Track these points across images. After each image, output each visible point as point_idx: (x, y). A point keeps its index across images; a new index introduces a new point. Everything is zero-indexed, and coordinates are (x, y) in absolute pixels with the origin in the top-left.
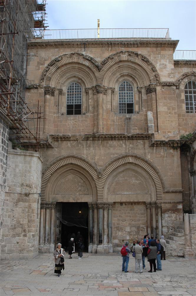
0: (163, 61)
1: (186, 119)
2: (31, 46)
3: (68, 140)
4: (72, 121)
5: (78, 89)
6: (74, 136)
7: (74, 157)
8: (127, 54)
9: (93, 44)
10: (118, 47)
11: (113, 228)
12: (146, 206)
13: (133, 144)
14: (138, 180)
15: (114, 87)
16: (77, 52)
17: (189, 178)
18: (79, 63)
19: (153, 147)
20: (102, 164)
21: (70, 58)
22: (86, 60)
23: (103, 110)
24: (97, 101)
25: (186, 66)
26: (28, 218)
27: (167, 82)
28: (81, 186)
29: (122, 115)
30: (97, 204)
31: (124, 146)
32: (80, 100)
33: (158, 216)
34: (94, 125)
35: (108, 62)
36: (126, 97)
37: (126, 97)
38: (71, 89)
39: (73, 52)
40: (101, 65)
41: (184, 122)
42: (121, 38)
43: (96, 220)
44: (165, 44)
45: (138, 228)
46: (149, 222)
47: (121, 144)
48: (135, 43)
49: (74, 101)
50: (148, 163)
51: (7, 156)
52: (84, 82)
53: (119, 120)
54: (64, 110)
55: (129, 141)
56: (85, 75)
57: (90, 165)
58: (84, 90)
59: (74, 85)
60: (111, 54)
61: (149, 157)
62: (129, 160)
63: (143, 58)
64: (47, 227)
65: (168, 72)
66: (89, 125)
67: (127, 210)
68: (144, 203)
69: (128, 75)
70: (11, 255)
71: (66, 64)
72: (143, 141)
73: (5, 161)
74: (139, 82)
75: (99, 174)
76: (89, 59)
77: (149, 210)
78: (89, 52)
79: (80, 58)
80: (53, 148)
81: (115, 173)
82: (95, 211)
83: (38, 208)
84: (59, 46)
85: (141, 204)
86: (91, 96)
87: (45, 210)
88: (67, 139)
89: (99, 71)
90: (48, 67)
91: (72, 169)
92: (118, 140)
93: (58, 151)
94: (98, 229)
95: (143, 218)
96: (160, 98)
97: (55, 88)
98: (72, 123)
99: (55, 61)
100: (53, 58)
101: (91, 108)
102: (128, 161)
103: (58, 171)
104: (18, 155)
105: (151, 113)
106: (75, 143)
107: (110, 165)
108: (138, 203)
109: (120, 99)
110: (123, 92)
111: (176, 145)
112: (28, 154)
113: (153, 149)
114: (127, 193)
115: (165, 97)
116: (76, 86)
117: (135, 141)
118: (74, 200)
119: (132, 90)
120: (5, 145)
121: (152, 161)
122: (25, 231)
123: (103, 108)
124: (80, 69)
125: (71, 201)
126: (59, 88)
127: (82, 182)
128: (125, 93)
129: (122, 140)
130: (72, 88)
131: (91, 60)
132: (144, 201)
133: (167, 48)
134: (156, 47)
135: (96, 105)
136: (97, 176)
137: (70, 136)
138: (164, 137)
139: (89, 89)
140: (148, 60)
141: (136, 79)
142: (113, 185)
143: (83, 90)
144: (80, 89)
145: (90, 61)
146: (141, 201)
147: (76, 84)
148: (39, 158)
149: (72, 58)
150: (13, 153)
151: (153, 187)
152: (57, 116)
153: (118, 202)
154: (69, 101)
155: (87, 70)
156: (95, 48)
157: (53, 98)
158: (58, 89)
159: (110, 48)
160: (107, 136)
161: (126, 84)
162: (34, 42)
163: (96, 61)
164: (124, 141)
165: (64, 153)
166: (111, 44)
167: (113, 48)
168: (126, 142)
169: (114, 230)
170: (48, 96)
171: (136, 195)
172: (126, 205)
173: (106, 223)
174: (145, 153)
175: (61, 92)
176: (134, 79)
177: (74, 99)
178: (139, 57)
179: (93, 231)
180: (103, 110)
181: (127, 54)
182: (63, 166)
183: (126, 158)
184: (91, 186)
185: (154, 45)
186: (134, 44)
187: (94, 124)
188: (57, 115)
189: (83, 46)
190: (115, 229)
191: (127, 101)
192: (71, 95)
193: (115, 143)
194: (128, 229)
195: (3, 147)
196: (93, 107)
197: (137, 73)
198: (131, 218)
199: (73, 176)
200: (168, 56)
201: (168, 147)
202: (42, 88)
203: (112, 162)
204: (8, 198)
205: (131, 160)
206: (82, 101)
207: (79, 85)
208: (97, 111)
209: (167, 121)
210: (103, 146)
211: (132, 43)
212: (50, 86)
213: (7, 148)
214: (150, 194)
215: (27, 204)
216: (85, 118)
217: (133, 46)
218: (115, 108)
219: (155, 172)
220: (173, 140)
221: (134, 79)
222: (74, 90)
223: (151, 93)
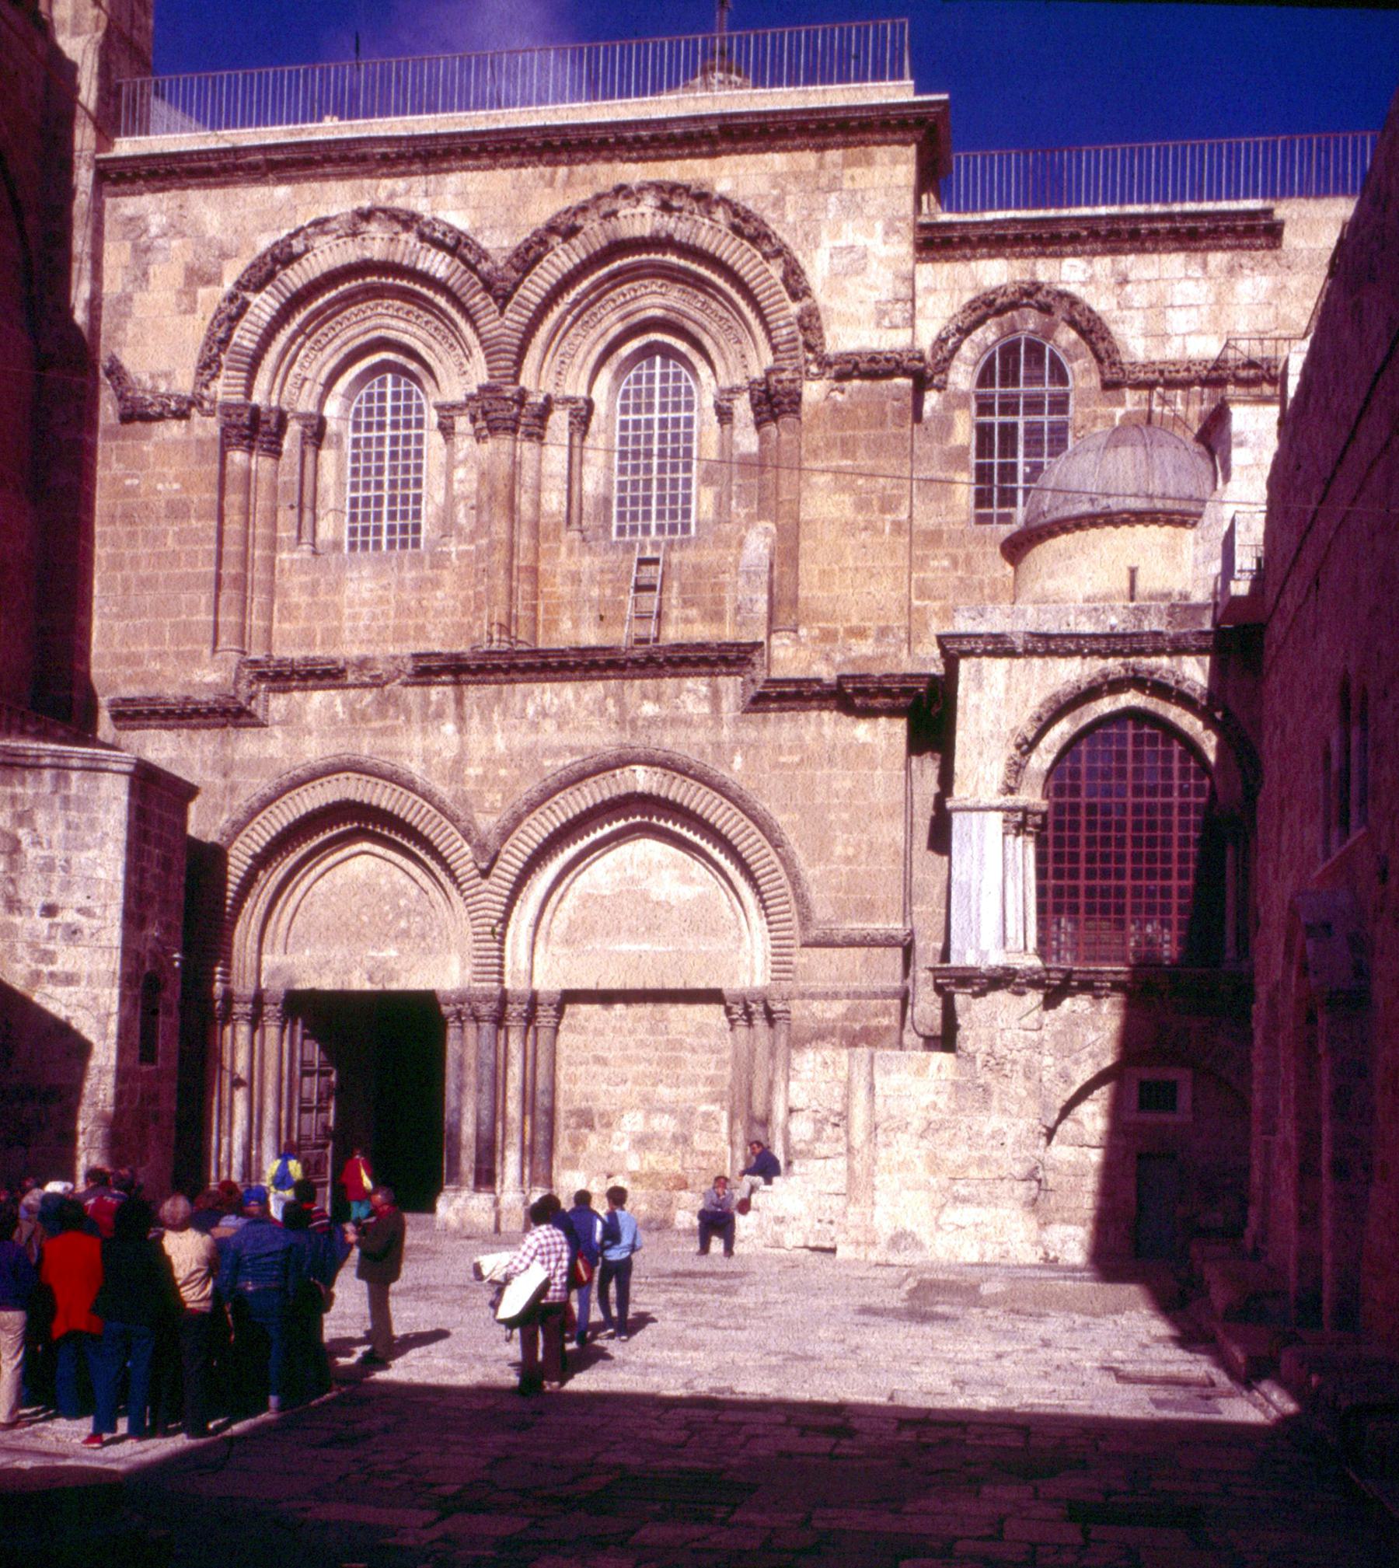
1: (968, 558)
6: (363, 664)
8: (650, 201)
13: (658, 699)
15: (582, 392)
16: (389, 204)
20: (499, 805)
21: (348, 240)
27: (859, 354)
35: (549, 256)
39: (366, 204)
41: (960, 573)
48: (694, 128)
56: (436, 329)
60: (567, 204)
62: (636, 781)
63: (737, 221)
66: (451, 602)
78: (449, 197)
81: (571, 852)
96: (818, 447)
101: (462, 515)
106: (369, 696)
107: (533, 806)
117: (669, 684)
119: (689, 406)
131: (456, 245)
137: (341, 664)
138: (828, 658)
139: (453, 407)
140: (762, 229)
144: (420, 409)
145: (452, 251)
159: (562, 171)
163: (484, 255)
165: (314, 750)
167: (581, 169)
177: (387, 463)
178: (720, 214)
183: (618, 772)
196: (472, 508)
197: (714, 305)
203: (548, 794)
205: (642, 779)
207: (415, 387)
209: (850, 574)
210: (504, 713)
216: (432, 568)
220: (861, 677)
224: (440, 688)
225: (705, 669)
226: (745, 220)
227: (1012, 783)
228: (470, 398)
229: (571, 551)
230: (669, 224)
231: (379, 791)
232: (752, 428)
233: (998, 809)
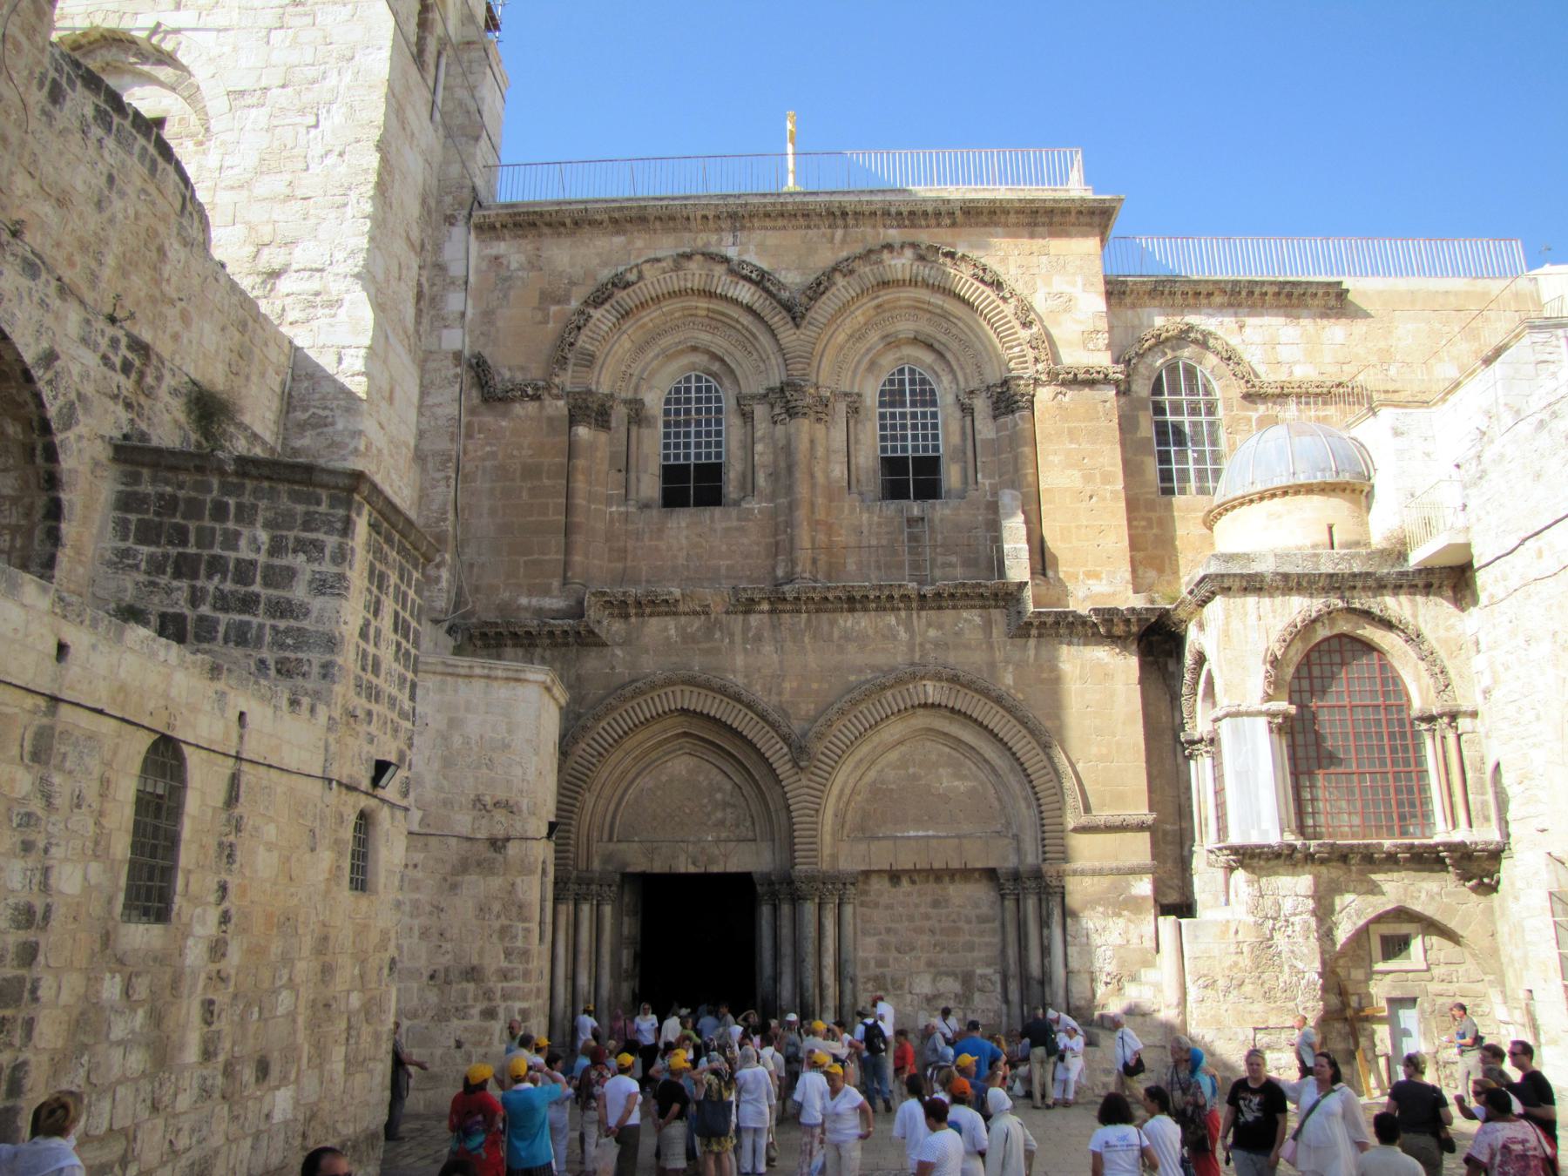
0: (1059, 284)
2: (517, 225)
3: (667, 614)
4: (685, 533)
5: (708, 400)
7: (691, 682)
9: (767, 215)
10: (874, 227)
11: (860, 980)
12: (1000, 888)
13: (940, 627)
14: (964, 778)
15: (856, 390)
17: (1177, 766)
18: (711, 295)
19: (1023, 641)
21: (674, 275)
22: (742, 282)
23: (813, 486)
24: (788, 450)
25: (1156, 302)
26: (502, 939)
28: (725, 805)
29: (892, 507)
30: (790, 882)
31: (903, 634)
32: (719, 444)
33: (1049, 927)
34: (775, 550)
35: (834, 289)
36: (909, 432)
37: (909, 432)
38: (678, 401)
39: (688, 250)
40: (804, 300)
42: (884, 191)
43: (786, 949)
44: (1066, 212)
45: (967, 979)
46: (1012, 953)
47: (890, 627)
48: (943, 209)
49: (693, 451)
50: (1003, 707)
51: (414, 686)
52: (732, 371)
53: (879, 525)
54: (650, 485)
55: (923, 613)
57: (763, 717)
58: (733, 402)
59: (693, 385)
60: (844, 254)
61: (1008, 679)
64: (584, 980)
65: (1083, 328)
66: (756, 548)
67: (917, 906)
68: (991, 874)
69: (916, 341)
70: (430, 1093)
71: (657, 300)
72: (984, 612)
73: (407, 705)
74: (962, 368)
75: (799, 752)
76: (754, 276)
77: (1010, 904)
79: (717, 274)
80: (605, 645)
81: (864, 749)
82: (786, 909)
83: (543, 900)
84: (629, 226)
85: (977, 881)
86: (762, 428)
87: (571, 907)
88: (664, 609)
89: (797, 326)
90: (583, 313)
91: (685, 734)
92: (876, 610)
93: (628, 658)
94: (799, 985)
95: (987, 939)
97: (612, 395)
98: (684, 541)
99: (614, 285)
100: (605, 274)
102: (922, 696)
103: (628, 744)
104: (459, 675)
105: (1014, 498)
106: (697, 623)
108: (965, 874)
109: (883, 438)
110: (898, 410)
111: (1119, 630)
112: (500, 673)
113: (1025, 647)
114: (921, 833)
115: (1070, 432)
116: (699, 390)
117: (948, 616)
118: (694, 863)
119: (934, 403)
120: (406, 637)
121: (1020, 696)
122: (488, 995)
123: (812, 476)
124: (716, 321)
125: (682, 870)
126: (630, 395)
127: (728, 786)
128: (903, 416)
129: (893, 609)
130: (683, 396)
131: (761, 280)
132: (991, 864)
133: (1073, 230)
134: (1029, 224)
135: (782, 464)
136: (789, 766)
139: (753, 397)
141: (949, 356)
142: (859, 798)
143: (729, 403)
144: (718, 400)
145: (757, 284)
146: (979, 865)
147: (699, 379)
148: (548, 689)
149: (681, 273)
150: (440, 668)
151: (1029, 807)
152: (621, 514)
153: (879, 872)
154: (672, 451)
155: (746, 320)
156: (777, 233)
157: (603, 437)
158: (626, 402)
159: (839, 233)
160: (830, 596)
161: (907, 377)
162: (528, 213)
163: (782, 286)
164: (903, 614)
166: (844, 214)
168: (910, 617)
169: (865, 990)
170: (582, 431)
171: (956, 841)
172: (913, 882)
173: (829, 961)
174: (992, 665)
175: (637, 415)
176: (941, 355)
177: (693, 440)
179: (776, 995)
180: (813, 486)
181: (909, 253)
182: (647, 722)
184: (767, 805)
185: (1024, 219)
186: (938, 214)
187: (777, 544)
188: (622, 509)
189: (726, 224)
190: (870, 986)
191: (915, 449)
192: (677, 424)
193: (862, 622)
194: (924, 986)
195: (398, 645)
198: (937, 937)
199: (692, 762)
200: (1078, 263)
201: (1086, 636)
202: (558, 397)
204: (419, 857)
205: (932, 691)
206: (728, 451)
207: (714, 383)
208: (790, 489)
211: (930, 209)
212: (594, 387)
213: (413, 651)
214: (1016, 837)
215: (496, 883)
216: (739, 519)
217: (933, 222)
218: (863, 478)
219: (1034, 744)
221: (941, 355)
222: (693, 406)
223: (1013, 412)
224: (758, 616)
225: (978, 602)
226: (984, 270)
227: (1271, 691)
228: (771, 390)
229: (852, 510)
230: (924, 271)
231: (709, 702)
232: (989, 421)
233: (1259, 713)
